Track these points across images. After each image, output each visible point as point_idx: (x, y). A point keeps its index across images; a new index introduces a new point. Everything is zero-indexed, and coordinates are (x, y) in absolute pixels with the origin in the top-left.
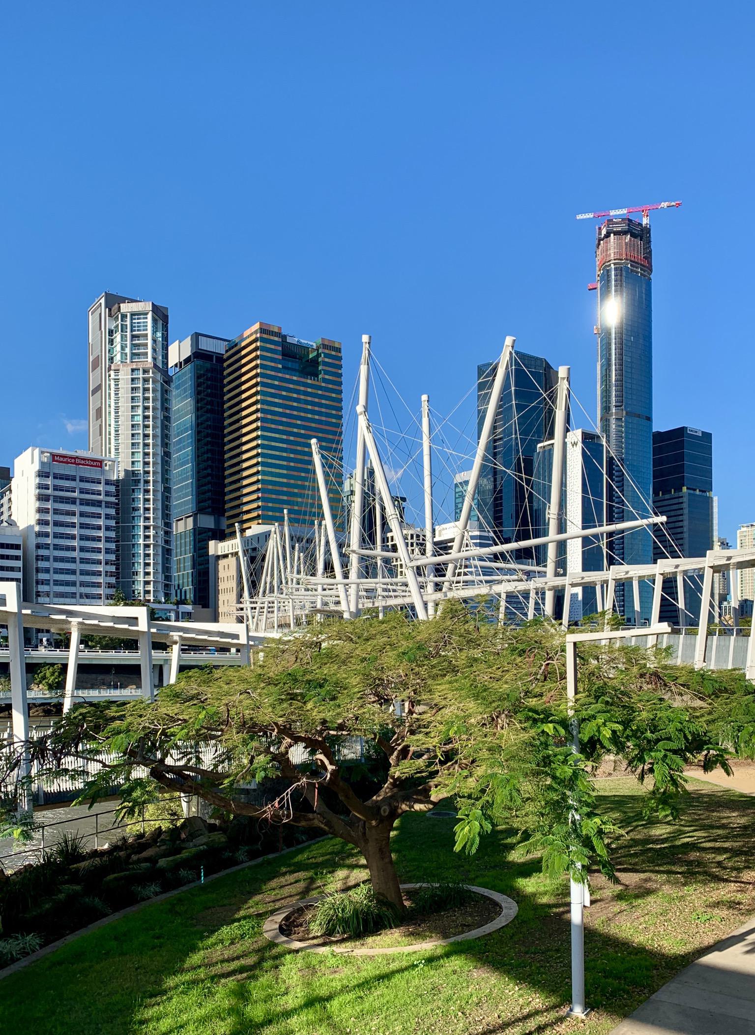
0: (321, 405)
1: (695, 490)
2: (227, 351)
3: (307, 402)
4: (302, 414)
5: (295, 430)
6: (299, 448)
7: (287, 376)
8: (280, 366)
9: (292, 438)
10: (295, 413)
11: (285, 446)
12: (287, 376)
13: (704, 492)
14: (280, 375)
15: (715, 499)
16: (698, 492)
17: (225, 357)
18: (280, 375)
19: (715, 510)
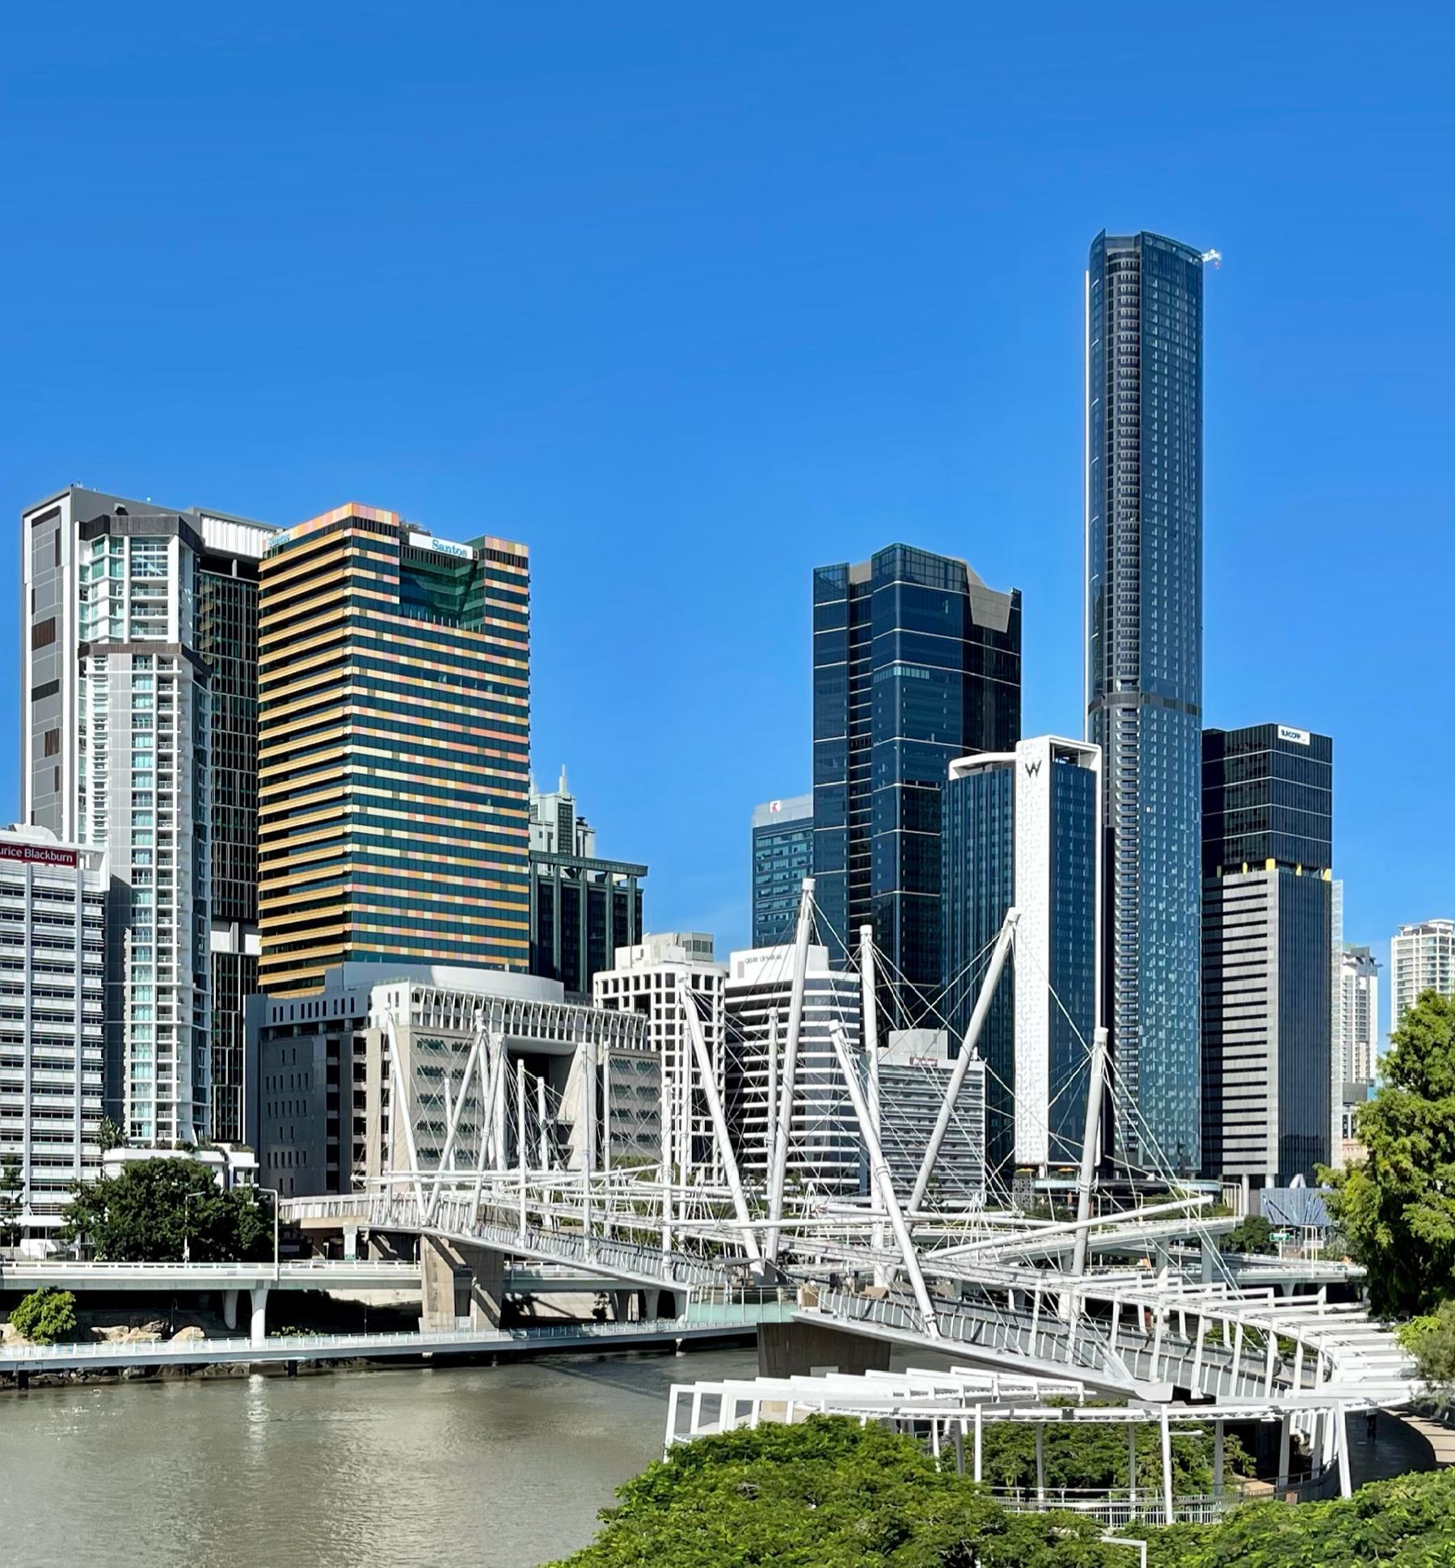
0: (482, 685)
1: (1293, 866)
2: (270, 554)
3: (453, 680)
4: (443, 706)
5: (427, 742)
6: (435, 782)
7: (412, 623)
8: (396, 600)
9: (420, 760)
10: (427, 703)
11: (404, 777)
12: (412, 623)
13: (1312, 869)
14: (396, 620)
15: (1338, 887)
16: (1299, 871)
17: (262, 568)
18: (396, 620)
19: (1338, 911)
